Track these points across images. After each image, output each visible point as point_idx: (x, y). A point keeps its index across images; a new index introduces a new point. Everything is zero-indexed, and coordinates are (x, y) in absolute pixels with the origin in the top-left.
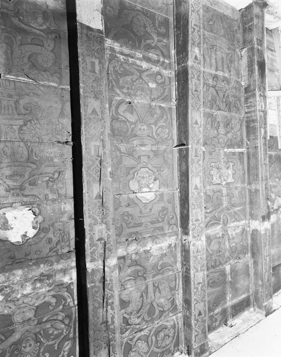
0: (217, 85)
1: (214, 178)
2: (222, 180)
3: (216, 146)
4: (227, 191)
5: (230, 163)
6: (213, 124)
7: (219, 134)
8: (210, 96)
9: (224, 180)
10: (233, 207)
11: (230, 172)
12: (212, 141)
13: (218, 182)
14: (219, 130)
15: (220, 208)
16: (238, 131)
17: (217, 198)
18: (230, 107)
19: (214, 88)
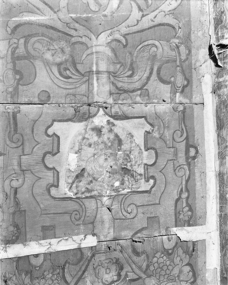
1: (139, 139)
2: (111, 131)
3: (130, 250)
4: (90, 91)
5: (70, 194)
9: (98, 131)
10: (59, 25)
11: (70, 161)
12: (148, 266)
13: (121, 126)
15: (125, 36)
17: (133, 69)
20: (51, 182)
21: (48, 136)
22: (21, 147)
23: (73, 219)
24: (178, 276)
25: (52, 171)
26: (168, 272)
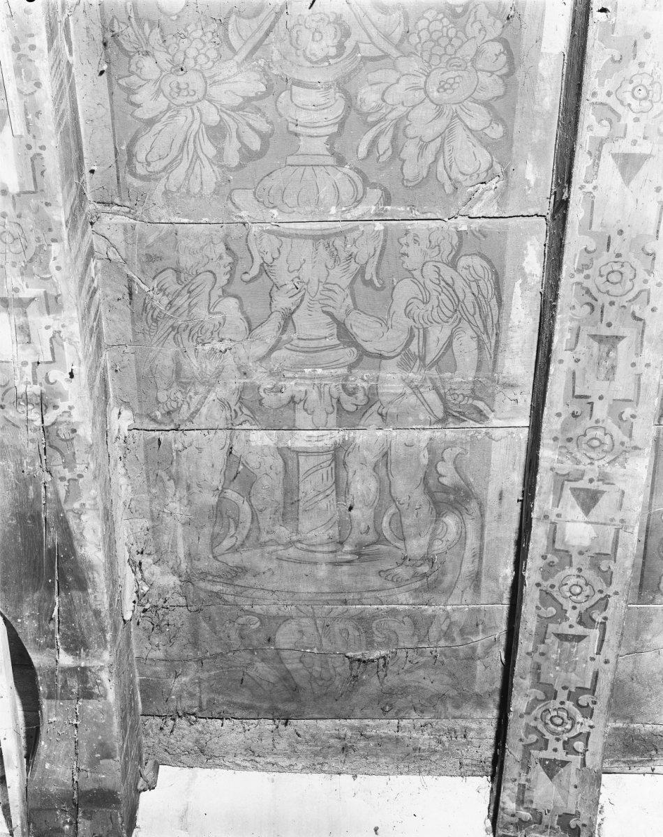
0: (344, 371)
6: (384, 143)
7: (344, 86)
8: (399, 306)
14: (338, 109)
16: (151, 122)
18: (233, 265)
19: (363, 353)
24: (473, 61)
26: (450, 50)
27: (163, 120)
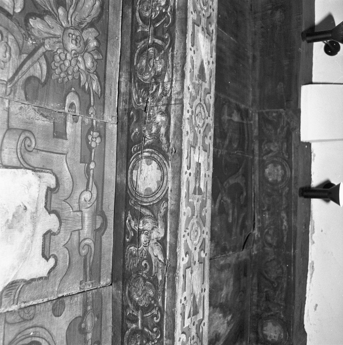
20: (54, 196)
21: (55, 257)
22: (82, 239)
23: (33, 140)
25: (52, 209)
27: (85, 24)
